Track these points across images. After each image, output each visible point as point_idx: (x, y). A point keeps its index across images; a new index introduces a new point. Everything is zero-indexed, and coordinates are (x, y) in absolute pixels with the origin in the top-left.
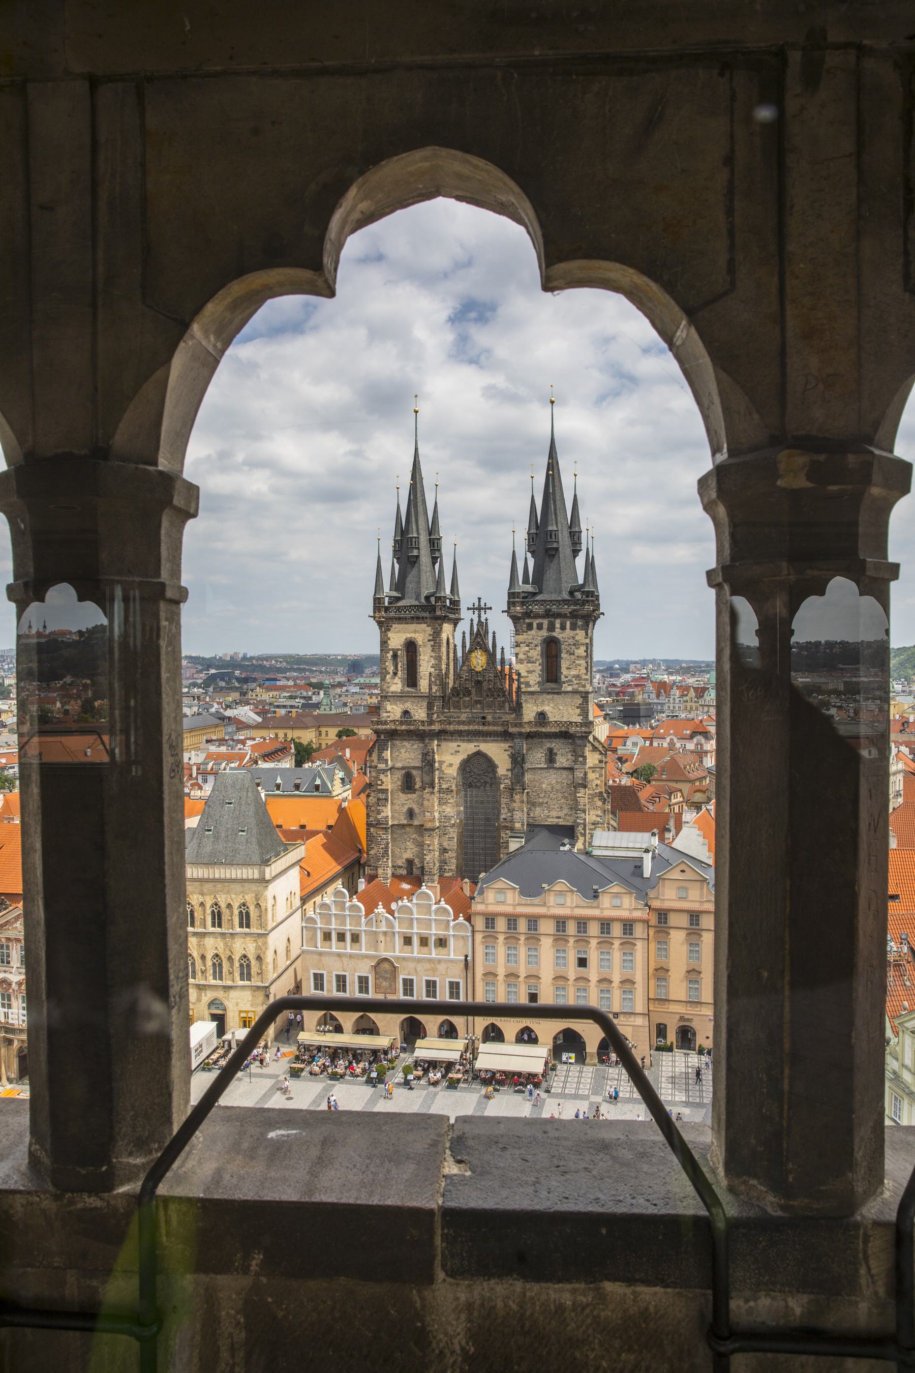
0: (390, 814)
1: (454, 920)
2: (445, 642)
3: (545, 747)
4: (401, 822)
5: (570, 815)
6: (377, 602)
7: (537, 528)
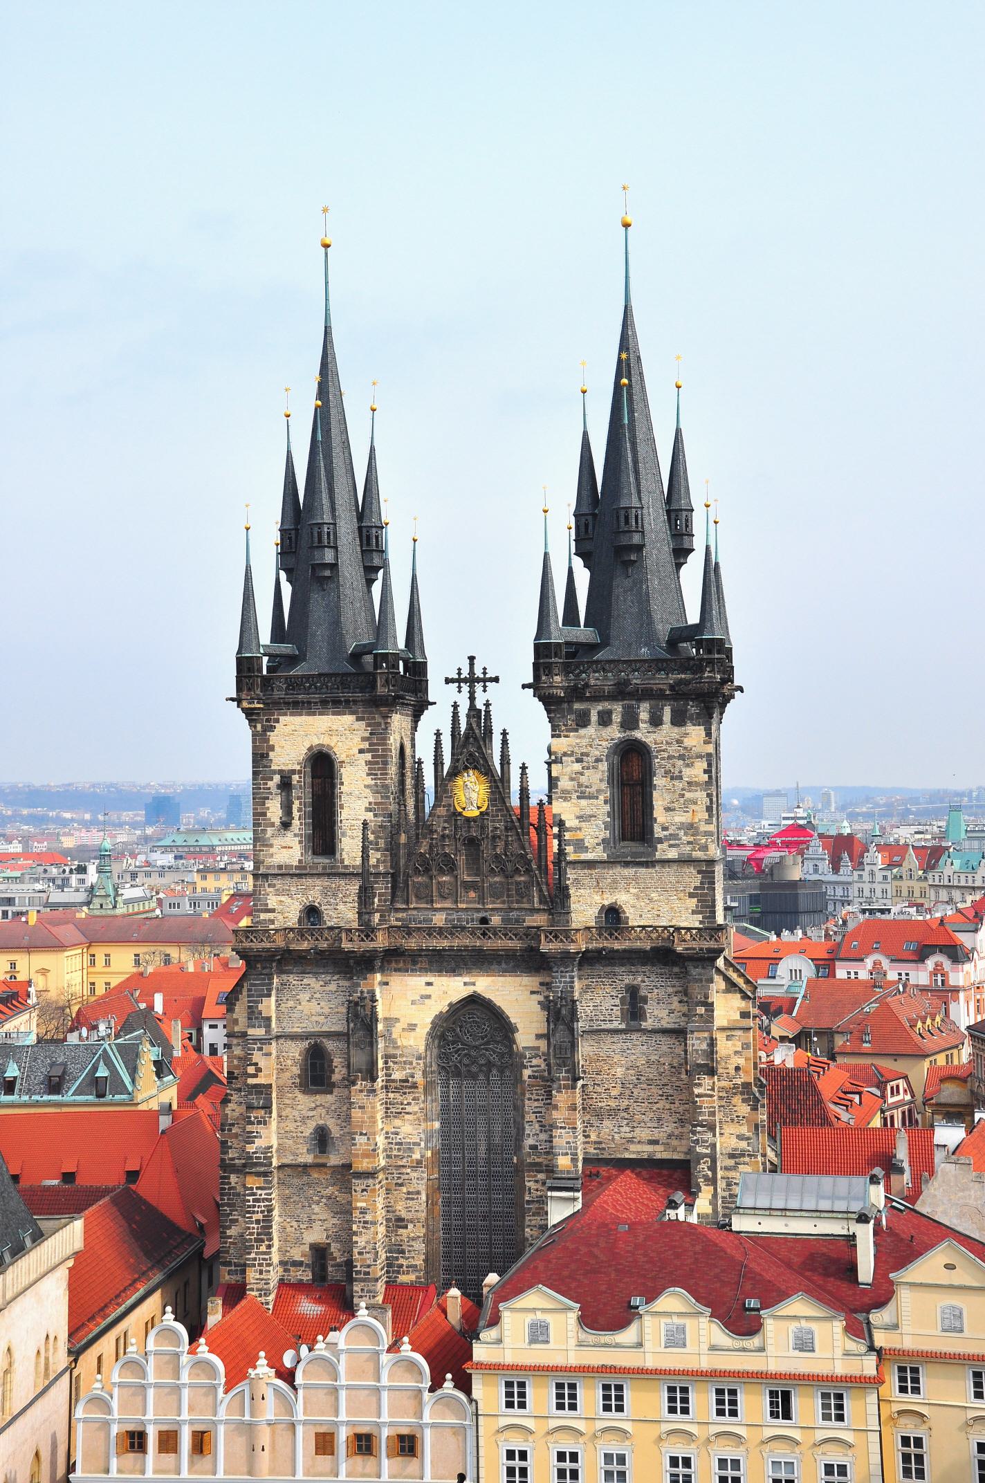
0: (274, 1142)
1: (432, 1390)
2: (395, 753)
4: (301, 1160)
5: (680, 1137)
6: (246, 667)
7: (595, 500)
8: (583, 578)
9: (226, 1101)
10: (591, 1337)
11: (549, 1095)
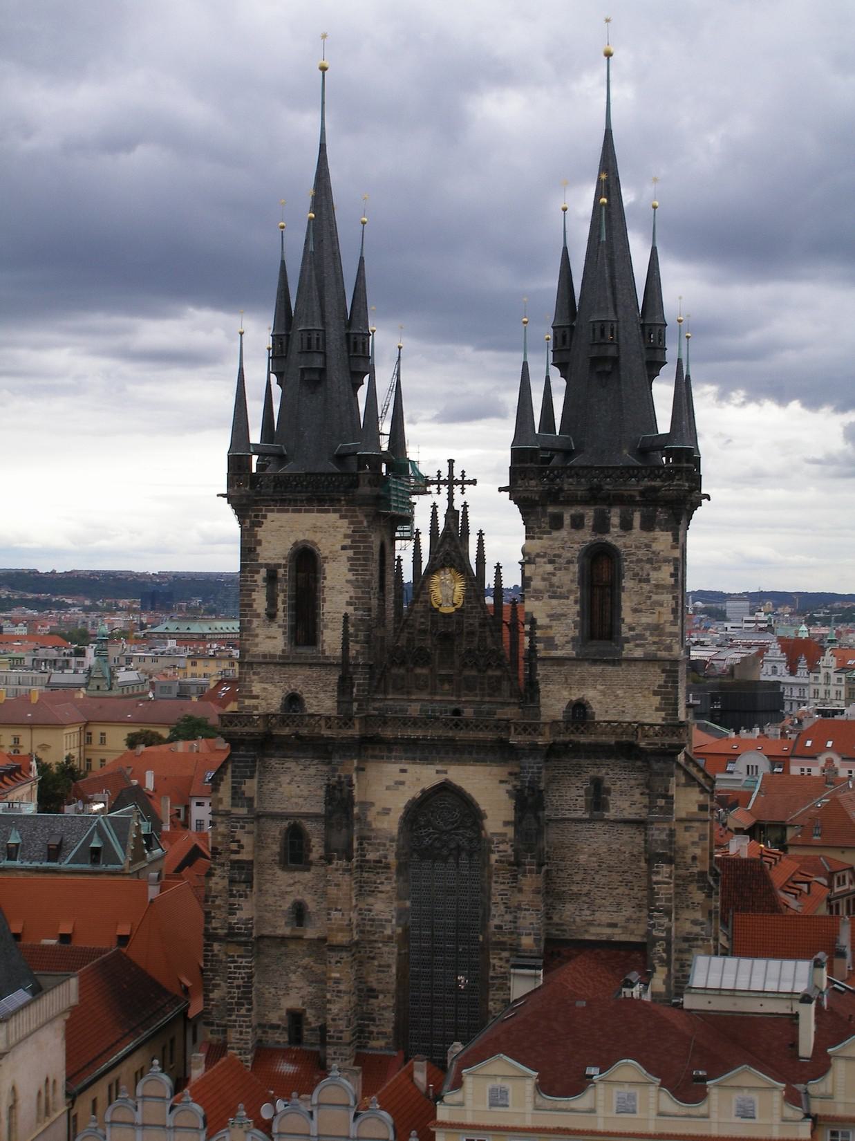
2: (376, 549)
3: (586, 777)
4: (280, 932)
5: (638, 921)
6: (237, 465)
8: (559, 385)
9: (210, 874)
10: (548, 1101)
11: (515, 878)
